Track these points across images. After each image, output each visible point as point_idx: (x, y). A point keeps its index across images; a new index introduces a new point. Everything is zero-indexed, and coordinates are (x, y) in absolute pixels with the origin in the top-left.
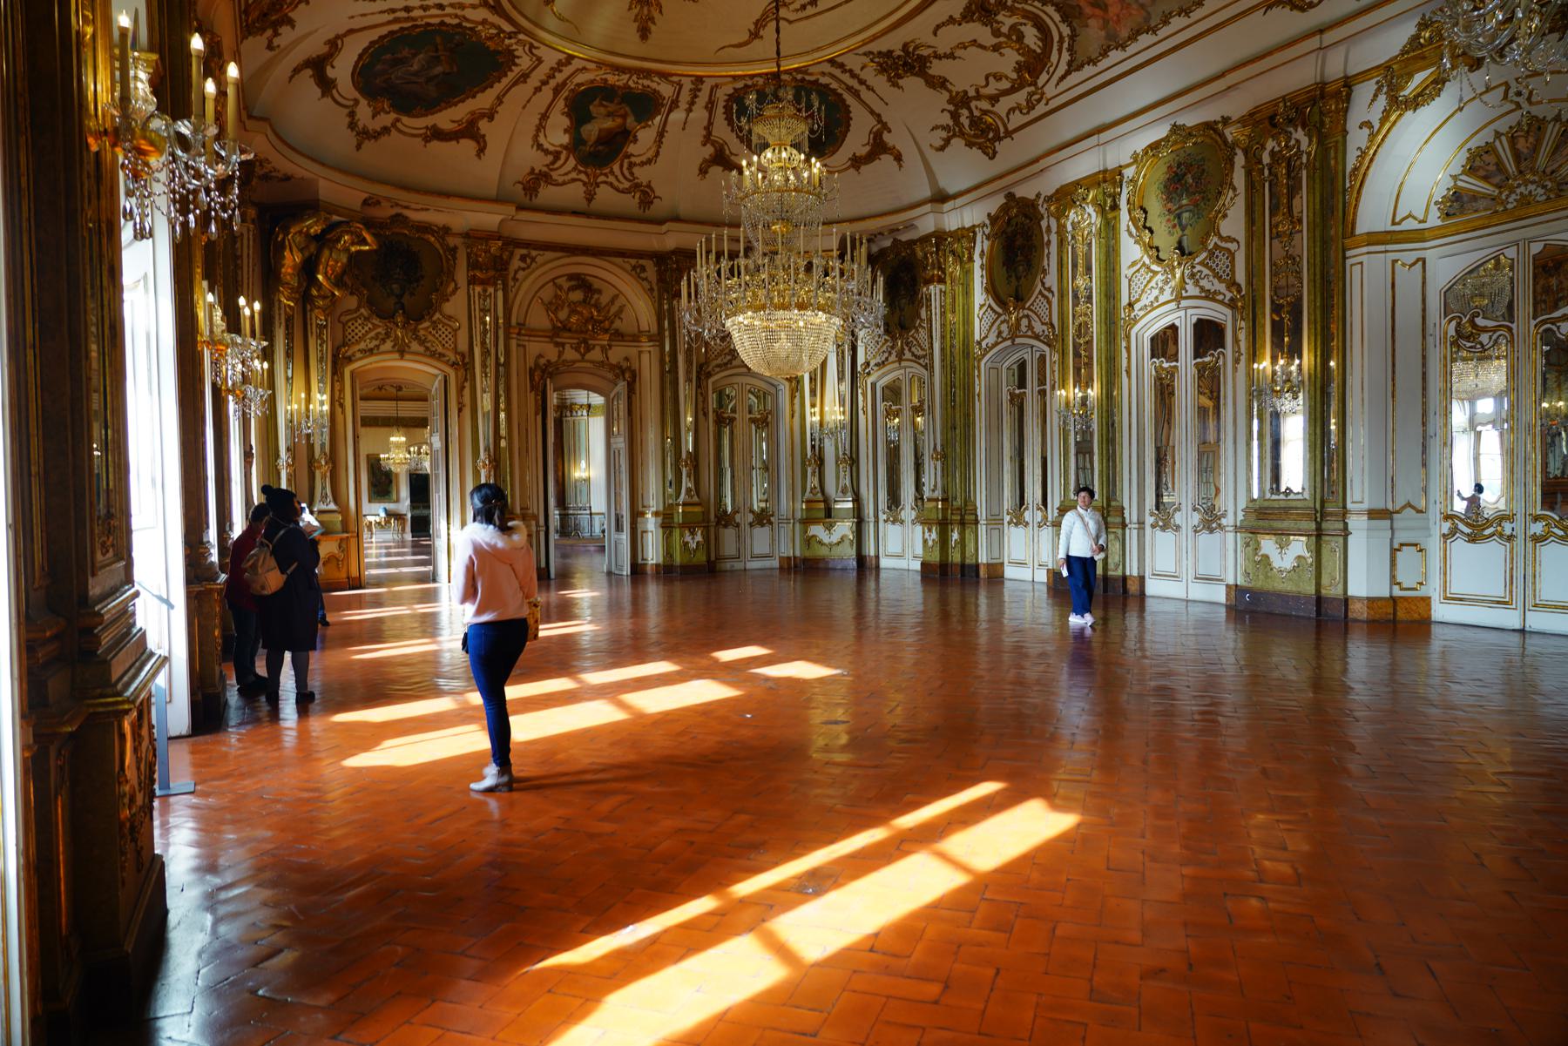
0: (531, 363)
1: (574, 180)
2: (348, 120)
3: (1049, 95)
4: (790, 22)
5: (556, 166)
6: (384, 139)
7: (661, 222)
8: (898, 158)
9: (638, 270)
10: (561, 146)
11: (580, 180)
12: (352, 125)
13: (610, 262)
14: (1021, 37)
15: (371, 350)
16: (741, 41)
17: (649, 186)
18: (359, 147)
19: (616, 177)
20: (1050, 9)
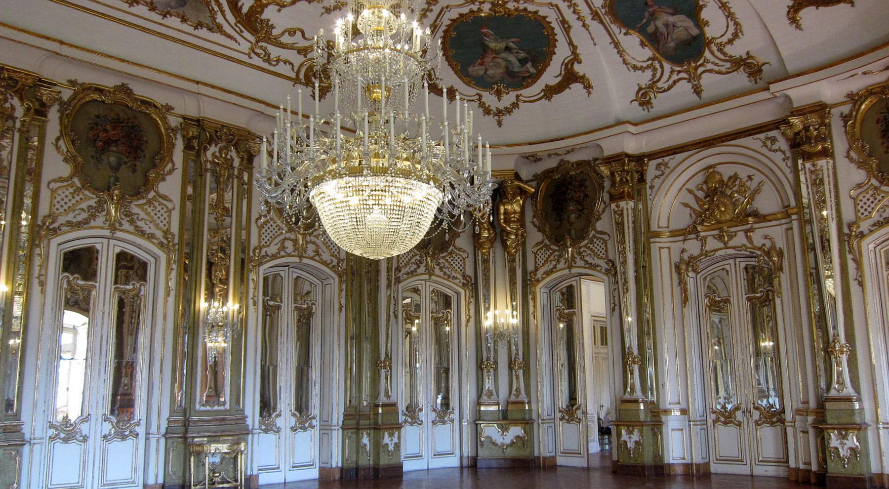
0: (676, 258)
1: (675, 82)
2: (481, 110)
6: (516, 111)
10: (648, 60)
12: (487, 111)
13: (728, 145)
18: (500, 124)
19: (713, 63)
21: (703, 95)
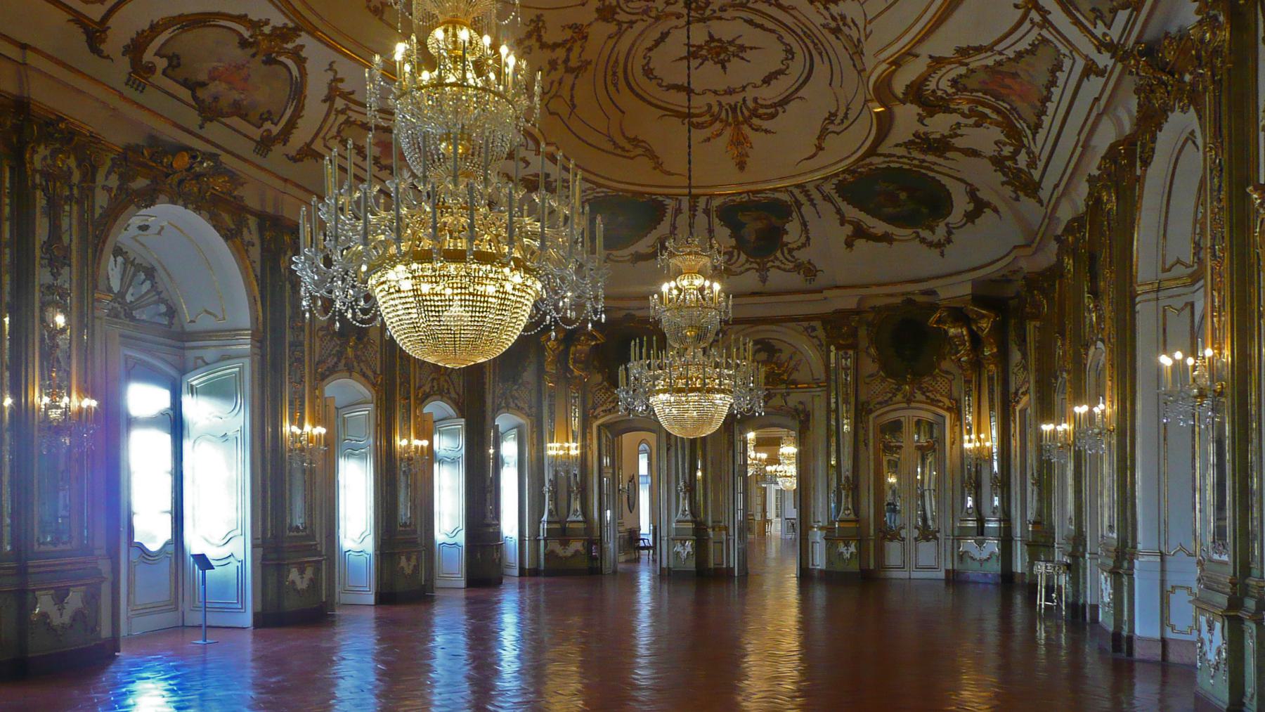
1: (748, 270)
3: (1037, 153)
4: (838, 133)
5: (733, 261)
7: (820, 291)
8: (996, 210)
9: (810, 330)
10: (732, 247)
11: (753, 268)
14: (985, 116)
15: (610, 410)
16: (812, 154)
17: (809, 262)
20: (980, 94)
21: (767, 283)
